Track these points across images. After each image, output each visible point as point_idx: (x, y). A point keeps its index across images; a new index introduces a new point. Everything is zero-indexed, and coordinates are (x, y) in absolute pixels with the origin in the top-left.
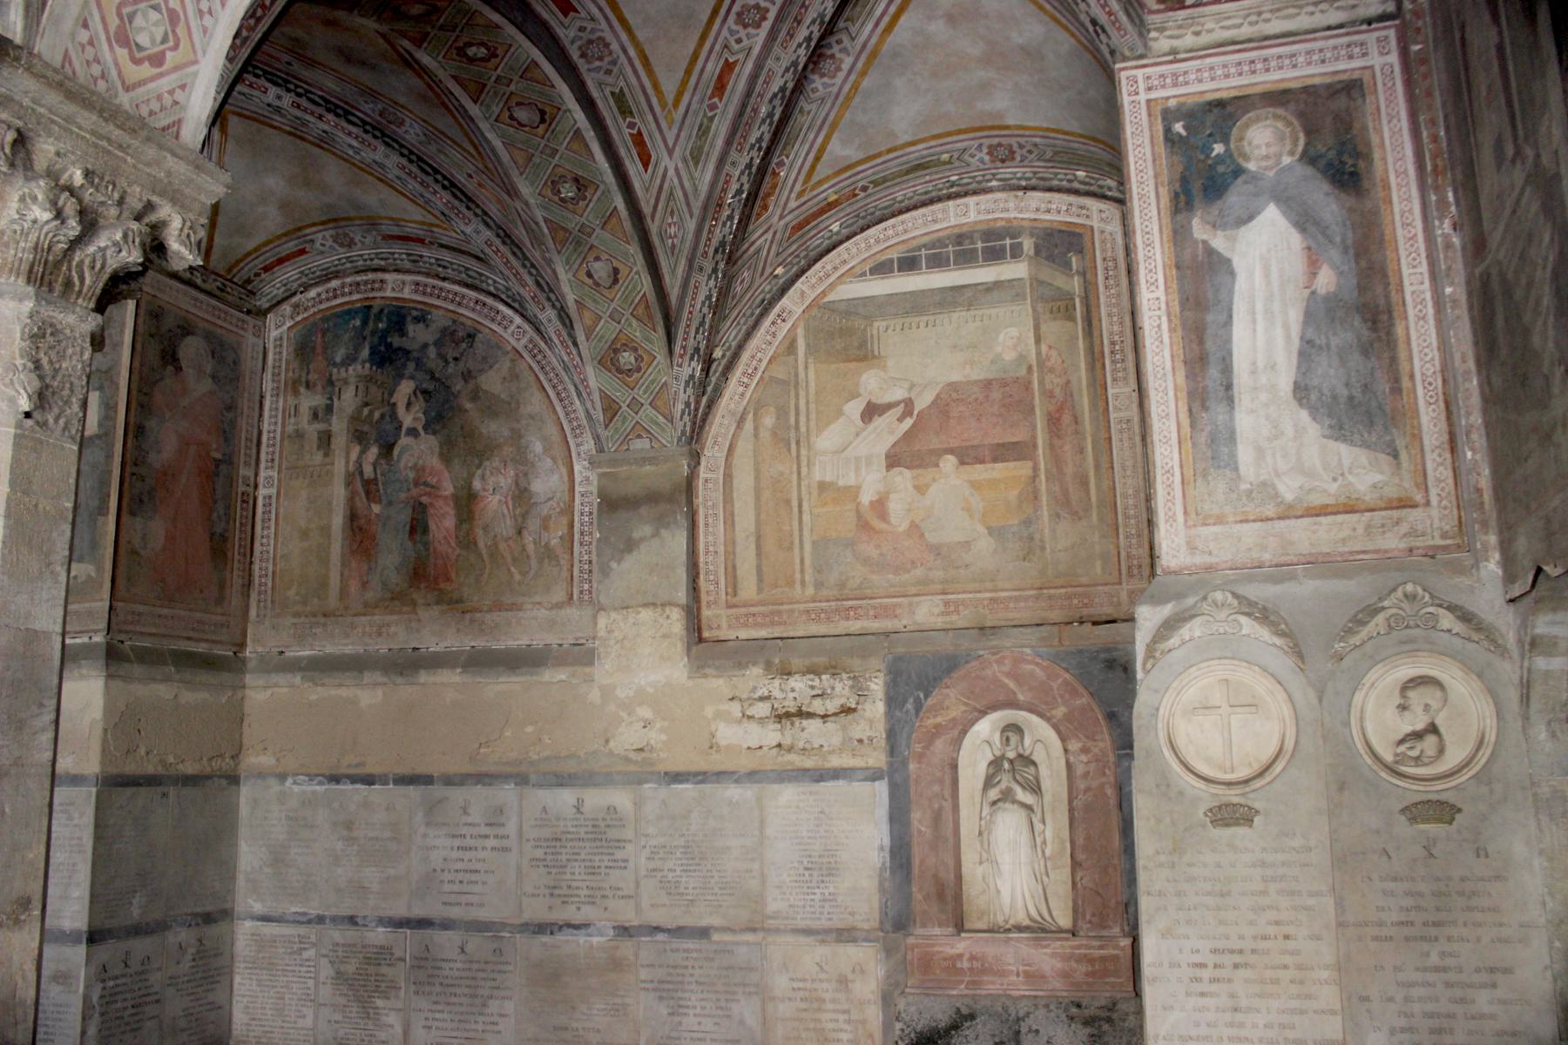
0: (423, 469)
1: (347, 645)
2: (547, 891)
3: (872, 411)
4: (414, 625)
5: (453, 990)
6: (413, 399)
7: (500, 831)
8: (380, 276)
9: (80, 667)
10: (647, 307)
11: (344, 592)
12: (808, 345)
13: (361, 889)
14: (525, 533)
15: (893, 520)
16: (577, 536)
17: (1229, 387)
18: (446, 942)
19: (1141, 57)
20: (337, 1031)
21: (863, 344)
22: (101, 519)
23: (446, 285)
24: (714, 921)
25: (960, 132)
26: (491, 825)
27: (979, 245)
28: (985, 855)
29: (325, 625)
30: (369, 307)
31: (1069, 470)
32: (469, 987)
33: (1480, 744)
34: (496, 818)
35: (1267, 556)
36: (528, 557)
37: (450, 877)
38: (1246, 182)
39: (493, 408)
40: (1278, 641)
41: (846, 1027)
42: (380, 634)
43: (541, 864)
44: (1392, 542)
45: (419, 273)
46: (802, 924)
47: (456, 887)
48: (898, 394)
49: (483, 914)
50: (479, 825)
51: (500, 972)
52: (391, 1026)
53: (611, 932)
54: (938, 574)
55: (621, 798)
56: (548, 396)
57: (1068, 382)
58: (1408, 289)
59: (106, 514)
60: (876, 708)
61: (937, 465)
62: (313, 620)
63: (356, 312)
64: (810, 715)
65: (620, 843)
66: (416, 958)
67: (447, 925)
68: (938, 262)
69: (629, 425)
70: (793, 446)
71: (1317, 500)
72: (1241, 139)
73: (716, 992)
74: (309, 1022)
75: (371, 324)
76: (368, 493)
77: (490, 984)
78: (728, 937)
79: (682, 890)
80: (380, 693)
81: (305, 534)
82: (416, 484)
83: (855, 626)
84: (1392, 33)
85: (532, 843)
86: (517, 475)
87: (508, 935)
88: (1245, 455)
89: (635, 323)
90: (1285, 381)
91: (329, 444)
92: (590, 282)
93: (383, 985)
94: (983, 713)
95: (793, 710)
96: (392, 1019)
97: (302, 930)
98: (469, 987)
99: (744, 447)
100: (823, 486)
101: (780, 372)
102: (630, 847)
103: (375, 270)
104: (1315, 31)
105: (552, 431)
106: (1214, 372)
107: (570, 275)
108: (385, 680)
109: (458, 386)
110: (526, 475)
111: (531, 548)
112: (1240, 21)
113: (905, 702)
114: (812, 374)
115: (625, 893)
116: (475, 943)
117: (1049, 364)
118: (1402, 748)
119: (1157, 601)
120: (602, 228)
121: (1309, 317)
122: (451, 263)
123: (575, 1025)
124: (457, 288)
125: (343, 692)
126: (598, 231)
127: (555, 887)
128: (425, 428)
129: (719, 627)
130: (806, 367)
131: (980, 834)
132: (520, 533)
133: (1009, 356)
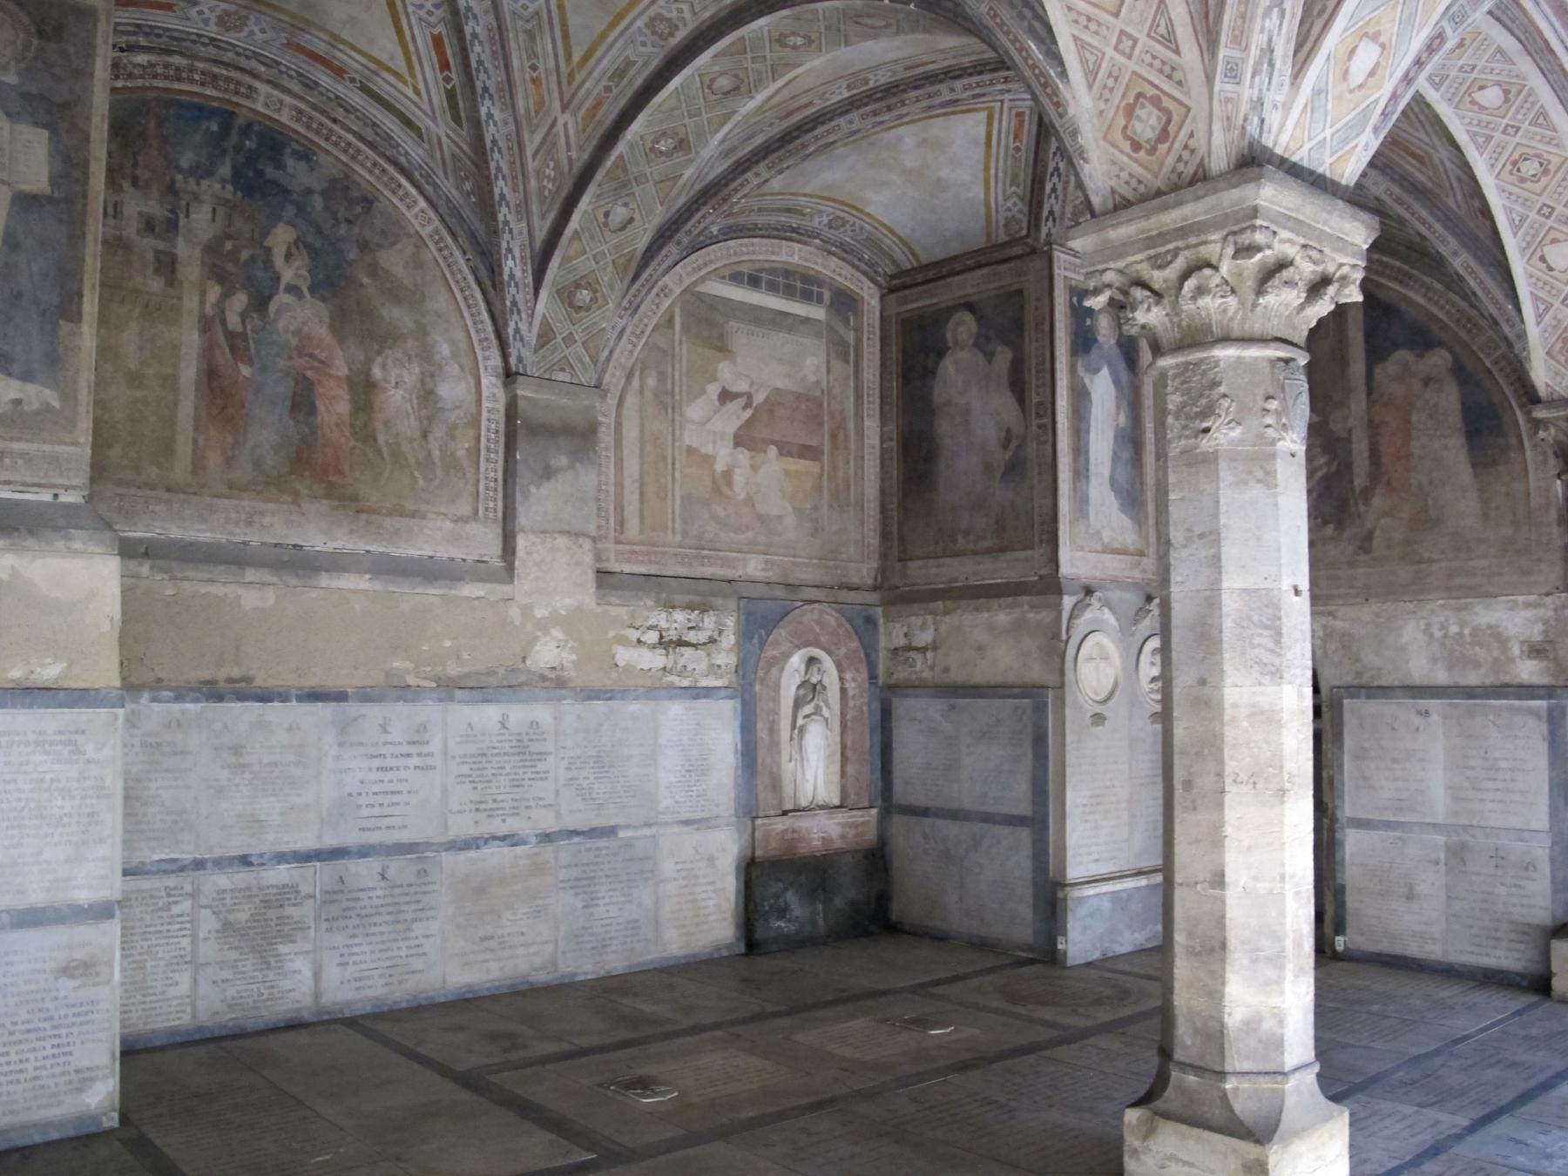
0: (309, 337)
1: (204, 531)
2: (473, 807)
3: (726, 396)
4: (296, 518)
5: (372, 920)
6: (294, 250)
7: (424, 749)
8: (247, 79)
9: (68, 538)
10: (630, 260)
11: (197, 466)
12: (682, 324)
13: (256, 823)
14: (431, 438)
15: (736, 489)
16: (483, 452)
17: (1087, 470)
18: (363, 871)
20: (225, 990)
21: (721, 337)
22: (65, 327)
23: (336, 128)
24: (621, 821)
25: (834, 201)
26: (414, 743)
27: (798, 284)
28: (795, 756)
29: (168, 502)
30: (232, 114)
31: (841, 474)
32: (389, 913)
34: (418, 737)
36: (434, 463)
37: (371, 800)
39: (396, 294)
41: (714, 895)
42: (250, 524)
43: (467, 780)
44: (1138, 575)
45: (302, 99)
46: (684, 816)
47: (376, 811)
48: (742, 387)
49: (405, 836)
50: (400, 743)
51: (425, 893)
52: (299, 972)
53: (533, 840)
54: (762, 539)
55: (541, 713)
56: (455, 299)
57: (843, 410)
59: (77, 318)
60: (729, 640)
61: (765, 452)
62: (152, 493)
63: (213, 112)
64: (688, 644)
65: (541, 756)
66: (328, 892)
67: (364, 852)
68: (773, 288)
69: (557, 356)
70: (670, 411)
71: (1116, 545)
73: (620, 882)
74: (184, 987)
75: (234, 138)
76: (233, 349)
77: (413, 907)
78: (630, 833)
79: (594, 796)
80: (271, 595)
81: (135, 380)
82: (301, 352)
83: (708, 571)
85: (458, 760)
86: (422, 373)
87: (432, 854)
89: (610, 268)
91: (173, 271)
92: (601, 219)
93: (286, 928)
94: (799, 647)
95: (674, 639)
96: (301, 967)
97: (171, 881)
98: (389, 913)
99: (632, 400)
100: (691, 451)
101: (660, 340)
102: (551, 759)
103: (242, 70)
105: (459, 335)
106: (1082, 459)
107: (590, 209)
108: (275, 580)
109: (353, 254)
110: (432, 375)
111: (436, 454)
113: (752, 638)
114: (685, 351)
115: (547, 802)
116: (399, 868)
117: (834, 392)
118: (1152, 686)
119: (1071, 594)
120: (655, 185)
121: (1116, 437)
122: (357, 110)
123: (500, 932)
124: (350, 138)
125: (219, 590)
126: (651, 183)
127: (481, 802)
128: (312, 289)
129: (608, 560)
130: (680, 344)
131: (792, 739)
132: (425, 435)
133: (812, 378)
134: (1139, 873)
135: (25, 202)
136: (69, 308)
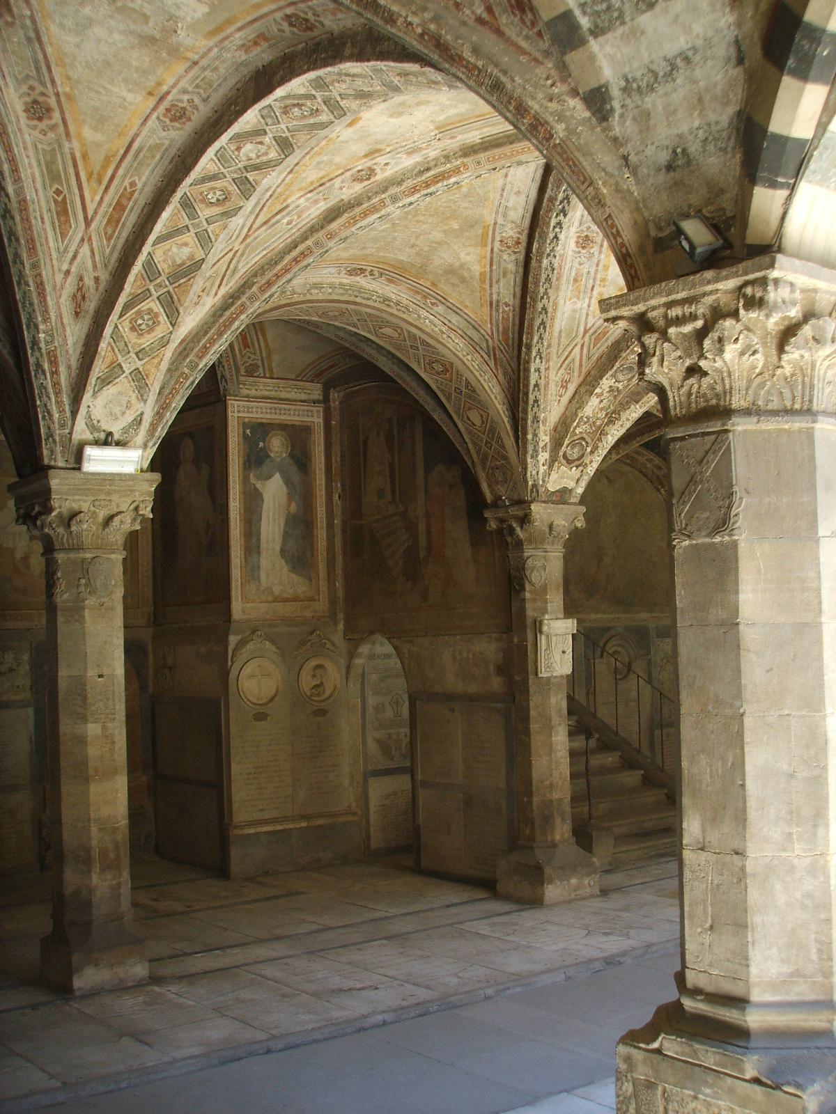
17: (259, 547)
19: (236, 396)
33: (335, 689)
35: (268, 616)
38: (270, 461)
40: (278, 651)
44: (308, 614)
58: (319, 516)
71: (285, 595)
72: (269, 442)
84: (321, 409)
88: (263, 575)
90: (278, 547)
104: (296, 401)
106: (254, 541)
112: (271, 388)
119: (236, 633)
134: (304, 817)
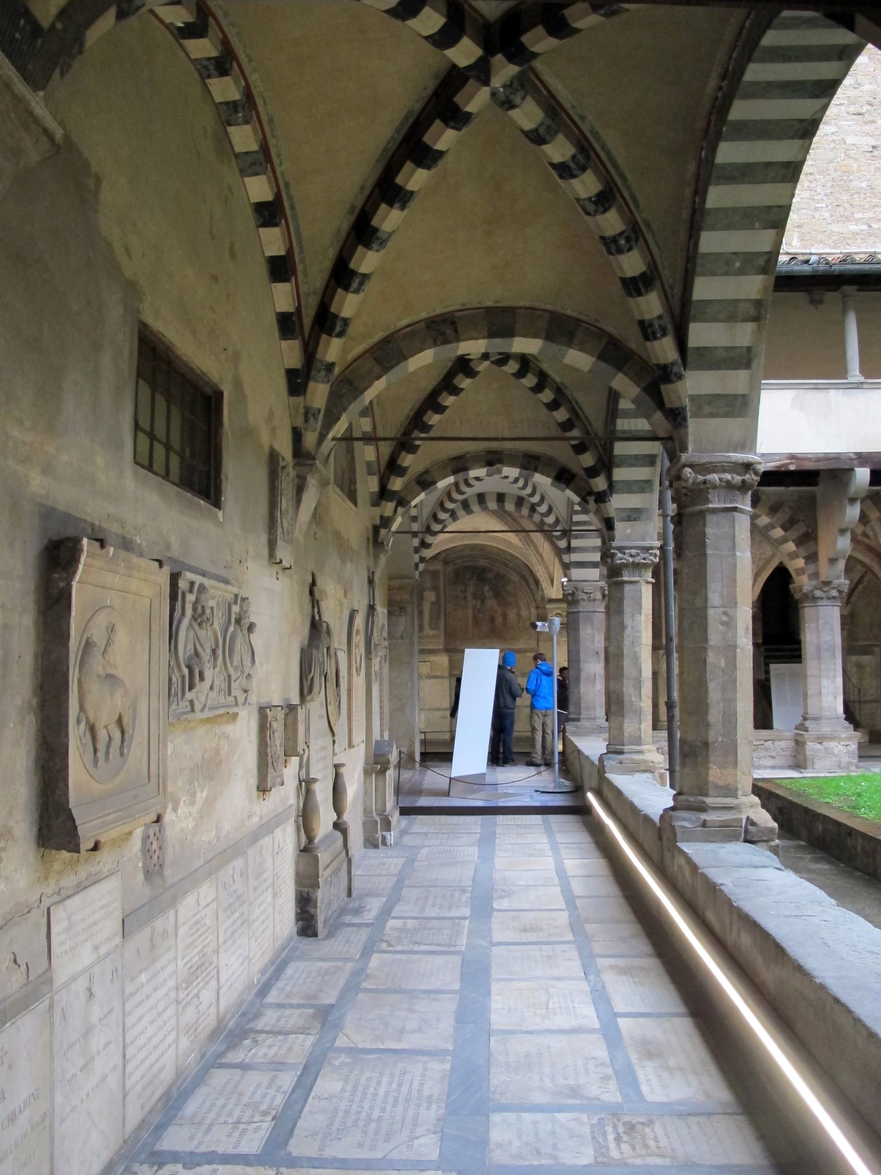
135: (432, 603)
136: (439, 618)
